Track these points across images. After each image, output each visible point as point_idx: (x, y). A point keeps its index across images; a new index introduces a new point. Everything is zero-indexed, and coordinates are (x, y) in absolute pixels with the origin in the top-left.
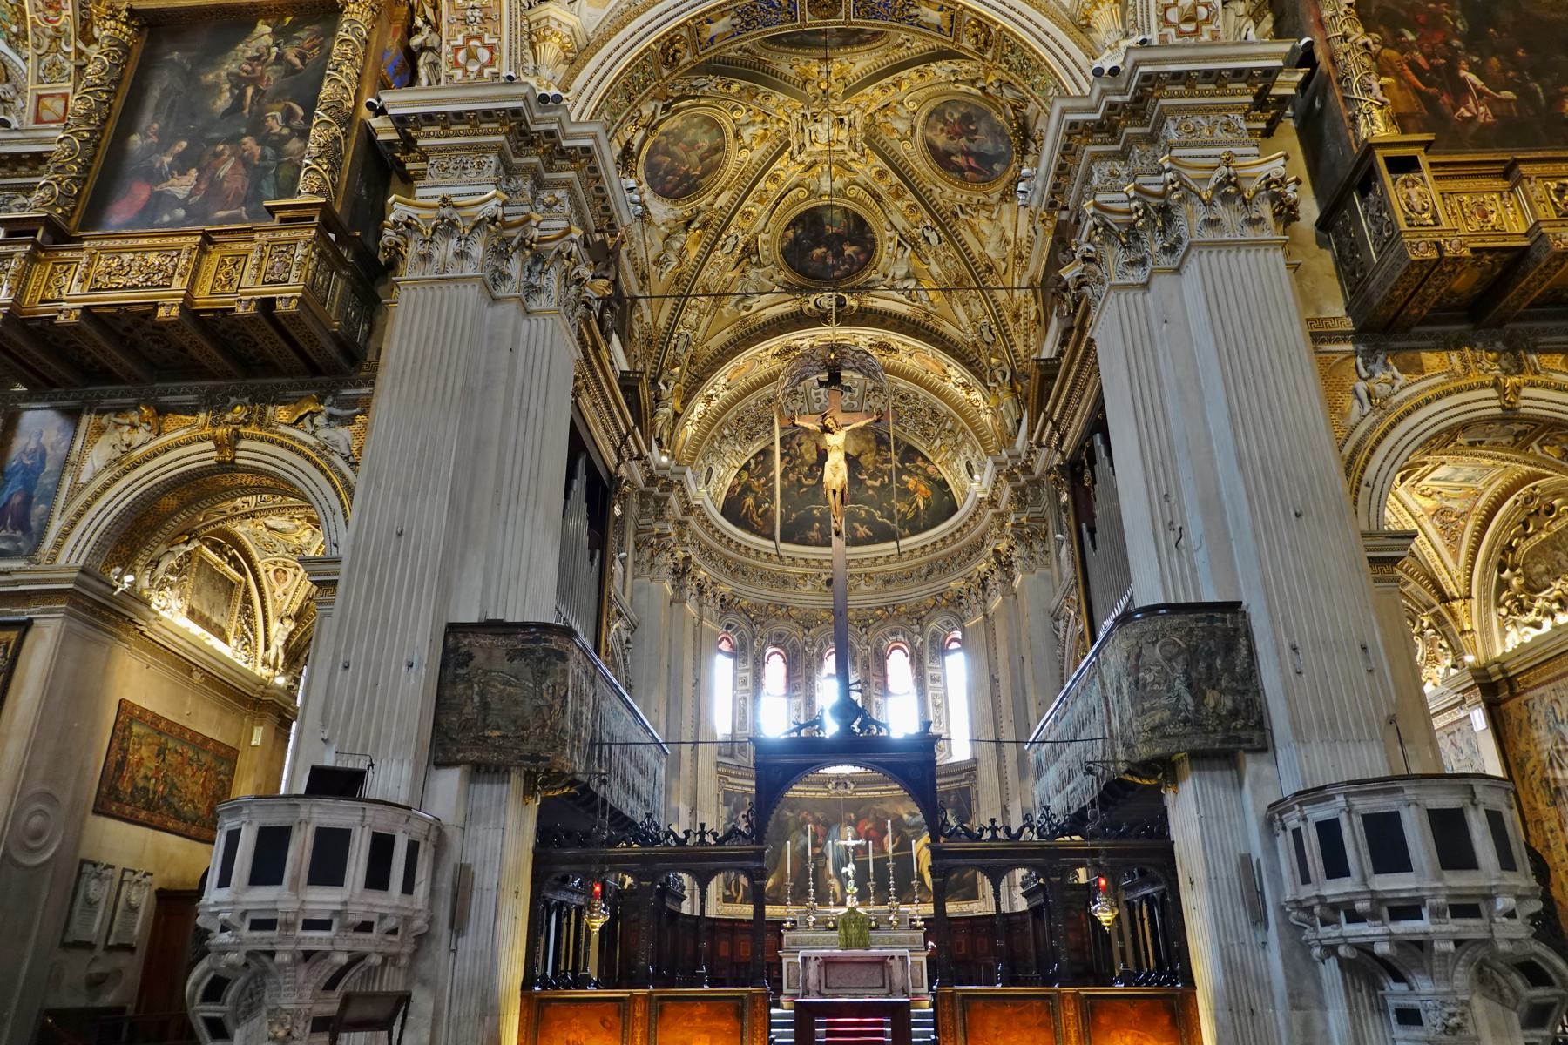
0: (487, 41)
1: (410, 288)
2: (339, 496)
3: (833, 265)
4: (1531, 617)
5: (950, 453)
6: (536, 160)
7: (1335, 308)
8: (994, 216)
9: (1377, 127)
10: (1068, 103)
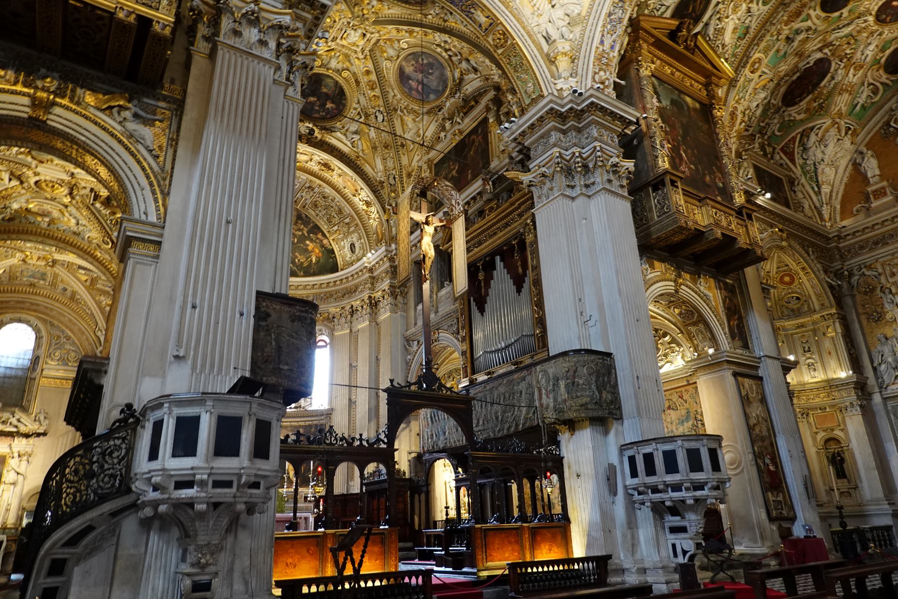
1: (226, 50)
2: (148, 177)
3: (317, 110)
5: (341, 236)
8: (417, 120)
9: (664, 164)
10: (554, 99)
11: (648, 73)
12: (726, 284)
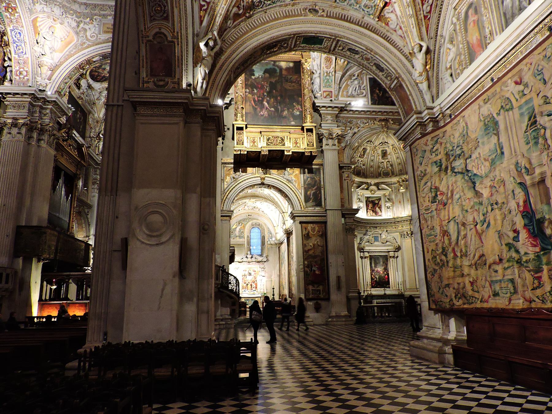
0: (25, 69)
6: (40, 104)
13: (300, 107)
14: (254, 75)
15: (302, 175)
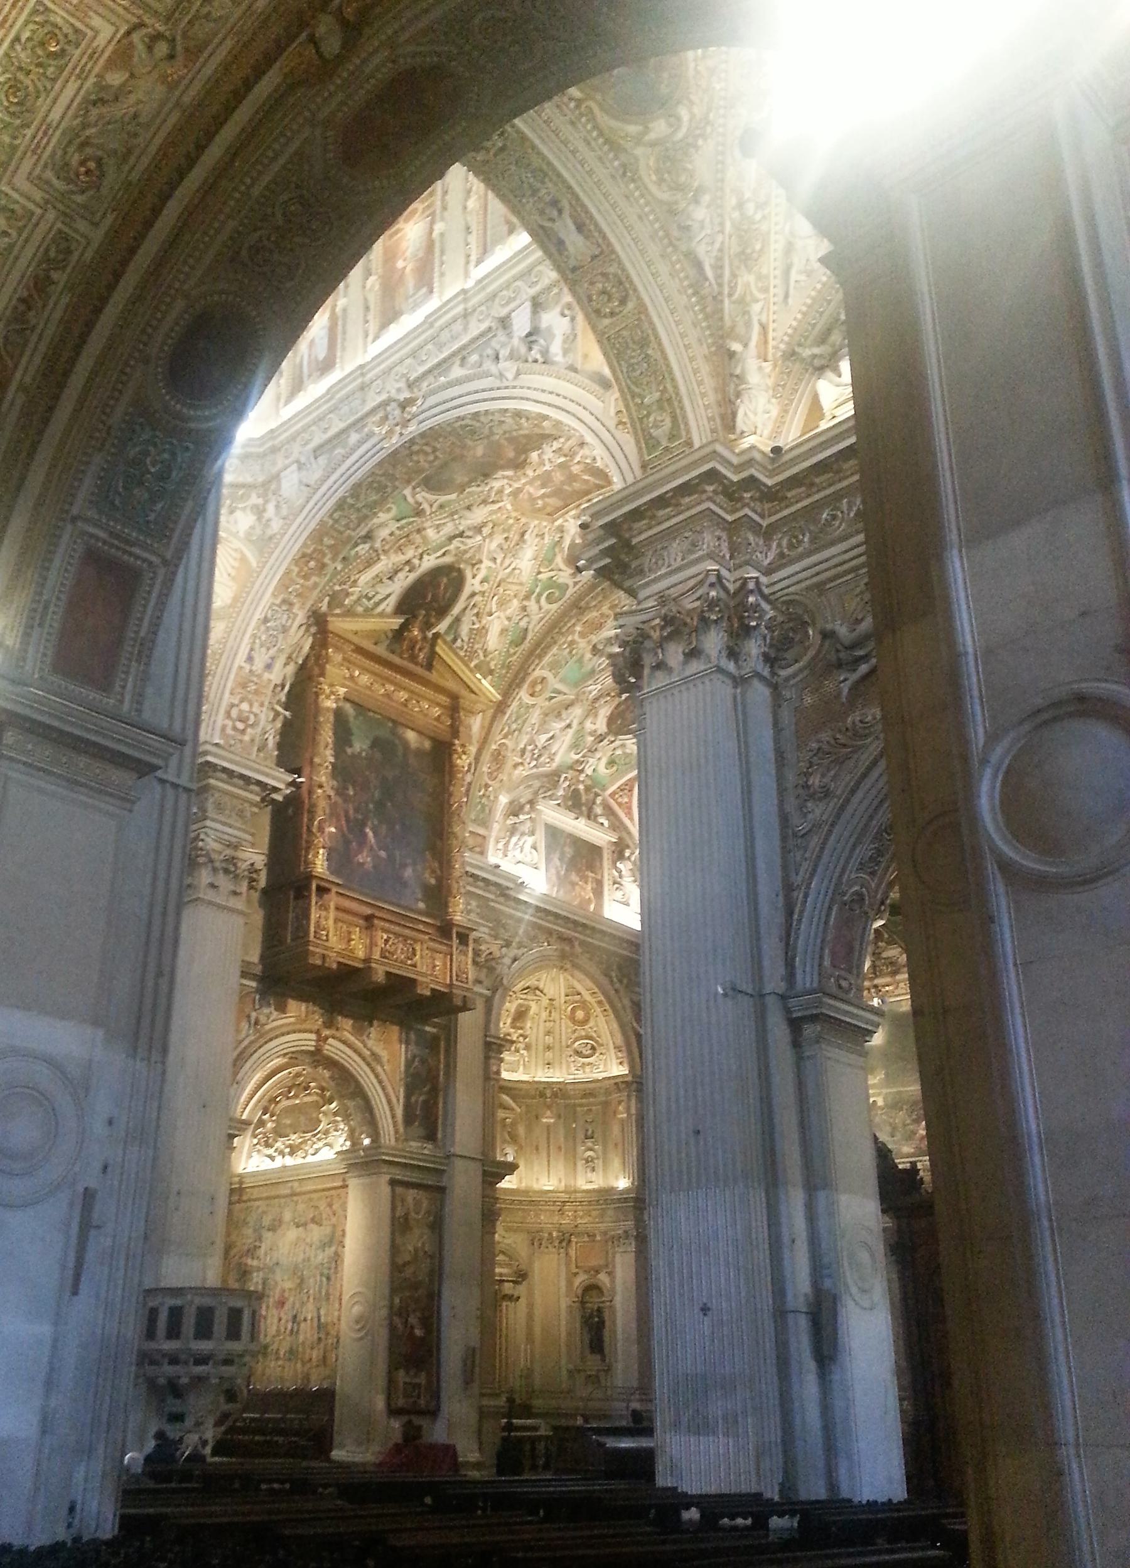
4: (271, 1151)
7: (254, 957)
11: (330, 704)
12: (421, 1034)
13: (436, 865)
14: (351, 746)
15: (403, 1046)
